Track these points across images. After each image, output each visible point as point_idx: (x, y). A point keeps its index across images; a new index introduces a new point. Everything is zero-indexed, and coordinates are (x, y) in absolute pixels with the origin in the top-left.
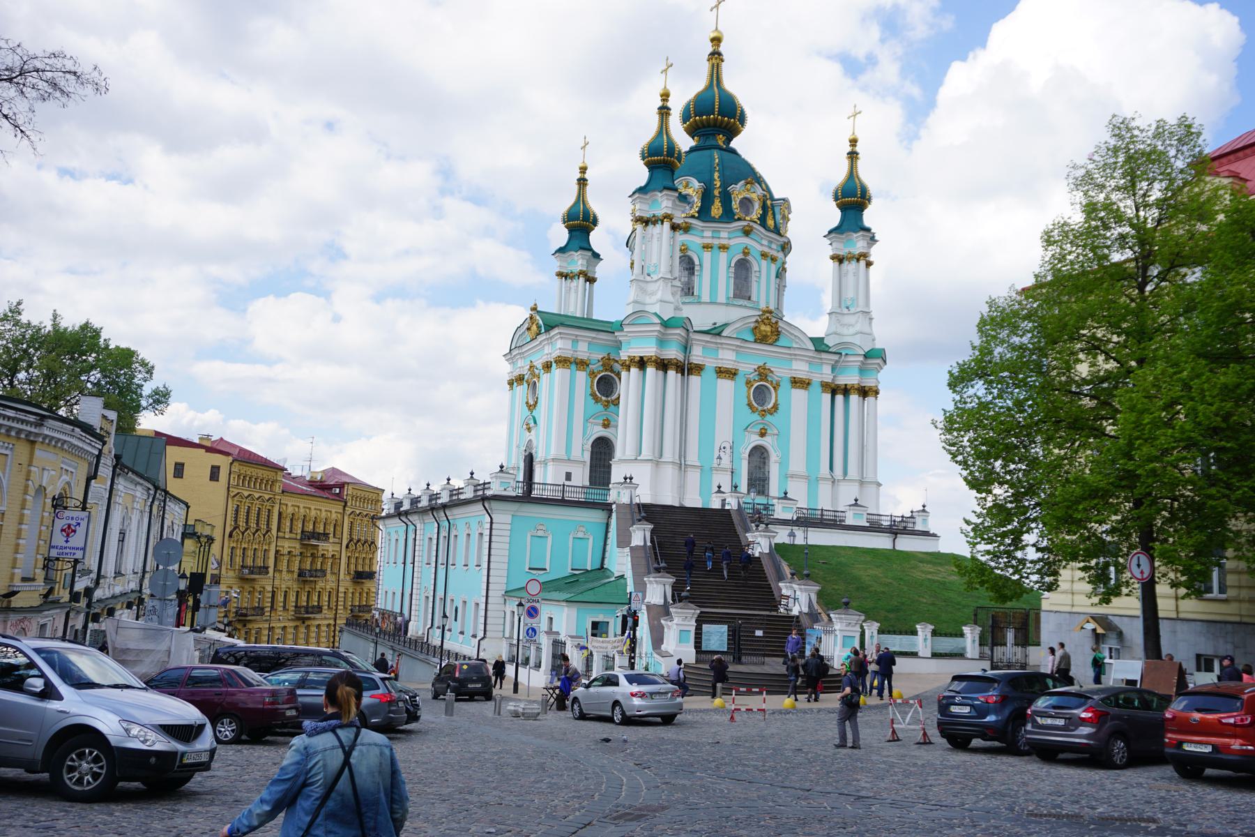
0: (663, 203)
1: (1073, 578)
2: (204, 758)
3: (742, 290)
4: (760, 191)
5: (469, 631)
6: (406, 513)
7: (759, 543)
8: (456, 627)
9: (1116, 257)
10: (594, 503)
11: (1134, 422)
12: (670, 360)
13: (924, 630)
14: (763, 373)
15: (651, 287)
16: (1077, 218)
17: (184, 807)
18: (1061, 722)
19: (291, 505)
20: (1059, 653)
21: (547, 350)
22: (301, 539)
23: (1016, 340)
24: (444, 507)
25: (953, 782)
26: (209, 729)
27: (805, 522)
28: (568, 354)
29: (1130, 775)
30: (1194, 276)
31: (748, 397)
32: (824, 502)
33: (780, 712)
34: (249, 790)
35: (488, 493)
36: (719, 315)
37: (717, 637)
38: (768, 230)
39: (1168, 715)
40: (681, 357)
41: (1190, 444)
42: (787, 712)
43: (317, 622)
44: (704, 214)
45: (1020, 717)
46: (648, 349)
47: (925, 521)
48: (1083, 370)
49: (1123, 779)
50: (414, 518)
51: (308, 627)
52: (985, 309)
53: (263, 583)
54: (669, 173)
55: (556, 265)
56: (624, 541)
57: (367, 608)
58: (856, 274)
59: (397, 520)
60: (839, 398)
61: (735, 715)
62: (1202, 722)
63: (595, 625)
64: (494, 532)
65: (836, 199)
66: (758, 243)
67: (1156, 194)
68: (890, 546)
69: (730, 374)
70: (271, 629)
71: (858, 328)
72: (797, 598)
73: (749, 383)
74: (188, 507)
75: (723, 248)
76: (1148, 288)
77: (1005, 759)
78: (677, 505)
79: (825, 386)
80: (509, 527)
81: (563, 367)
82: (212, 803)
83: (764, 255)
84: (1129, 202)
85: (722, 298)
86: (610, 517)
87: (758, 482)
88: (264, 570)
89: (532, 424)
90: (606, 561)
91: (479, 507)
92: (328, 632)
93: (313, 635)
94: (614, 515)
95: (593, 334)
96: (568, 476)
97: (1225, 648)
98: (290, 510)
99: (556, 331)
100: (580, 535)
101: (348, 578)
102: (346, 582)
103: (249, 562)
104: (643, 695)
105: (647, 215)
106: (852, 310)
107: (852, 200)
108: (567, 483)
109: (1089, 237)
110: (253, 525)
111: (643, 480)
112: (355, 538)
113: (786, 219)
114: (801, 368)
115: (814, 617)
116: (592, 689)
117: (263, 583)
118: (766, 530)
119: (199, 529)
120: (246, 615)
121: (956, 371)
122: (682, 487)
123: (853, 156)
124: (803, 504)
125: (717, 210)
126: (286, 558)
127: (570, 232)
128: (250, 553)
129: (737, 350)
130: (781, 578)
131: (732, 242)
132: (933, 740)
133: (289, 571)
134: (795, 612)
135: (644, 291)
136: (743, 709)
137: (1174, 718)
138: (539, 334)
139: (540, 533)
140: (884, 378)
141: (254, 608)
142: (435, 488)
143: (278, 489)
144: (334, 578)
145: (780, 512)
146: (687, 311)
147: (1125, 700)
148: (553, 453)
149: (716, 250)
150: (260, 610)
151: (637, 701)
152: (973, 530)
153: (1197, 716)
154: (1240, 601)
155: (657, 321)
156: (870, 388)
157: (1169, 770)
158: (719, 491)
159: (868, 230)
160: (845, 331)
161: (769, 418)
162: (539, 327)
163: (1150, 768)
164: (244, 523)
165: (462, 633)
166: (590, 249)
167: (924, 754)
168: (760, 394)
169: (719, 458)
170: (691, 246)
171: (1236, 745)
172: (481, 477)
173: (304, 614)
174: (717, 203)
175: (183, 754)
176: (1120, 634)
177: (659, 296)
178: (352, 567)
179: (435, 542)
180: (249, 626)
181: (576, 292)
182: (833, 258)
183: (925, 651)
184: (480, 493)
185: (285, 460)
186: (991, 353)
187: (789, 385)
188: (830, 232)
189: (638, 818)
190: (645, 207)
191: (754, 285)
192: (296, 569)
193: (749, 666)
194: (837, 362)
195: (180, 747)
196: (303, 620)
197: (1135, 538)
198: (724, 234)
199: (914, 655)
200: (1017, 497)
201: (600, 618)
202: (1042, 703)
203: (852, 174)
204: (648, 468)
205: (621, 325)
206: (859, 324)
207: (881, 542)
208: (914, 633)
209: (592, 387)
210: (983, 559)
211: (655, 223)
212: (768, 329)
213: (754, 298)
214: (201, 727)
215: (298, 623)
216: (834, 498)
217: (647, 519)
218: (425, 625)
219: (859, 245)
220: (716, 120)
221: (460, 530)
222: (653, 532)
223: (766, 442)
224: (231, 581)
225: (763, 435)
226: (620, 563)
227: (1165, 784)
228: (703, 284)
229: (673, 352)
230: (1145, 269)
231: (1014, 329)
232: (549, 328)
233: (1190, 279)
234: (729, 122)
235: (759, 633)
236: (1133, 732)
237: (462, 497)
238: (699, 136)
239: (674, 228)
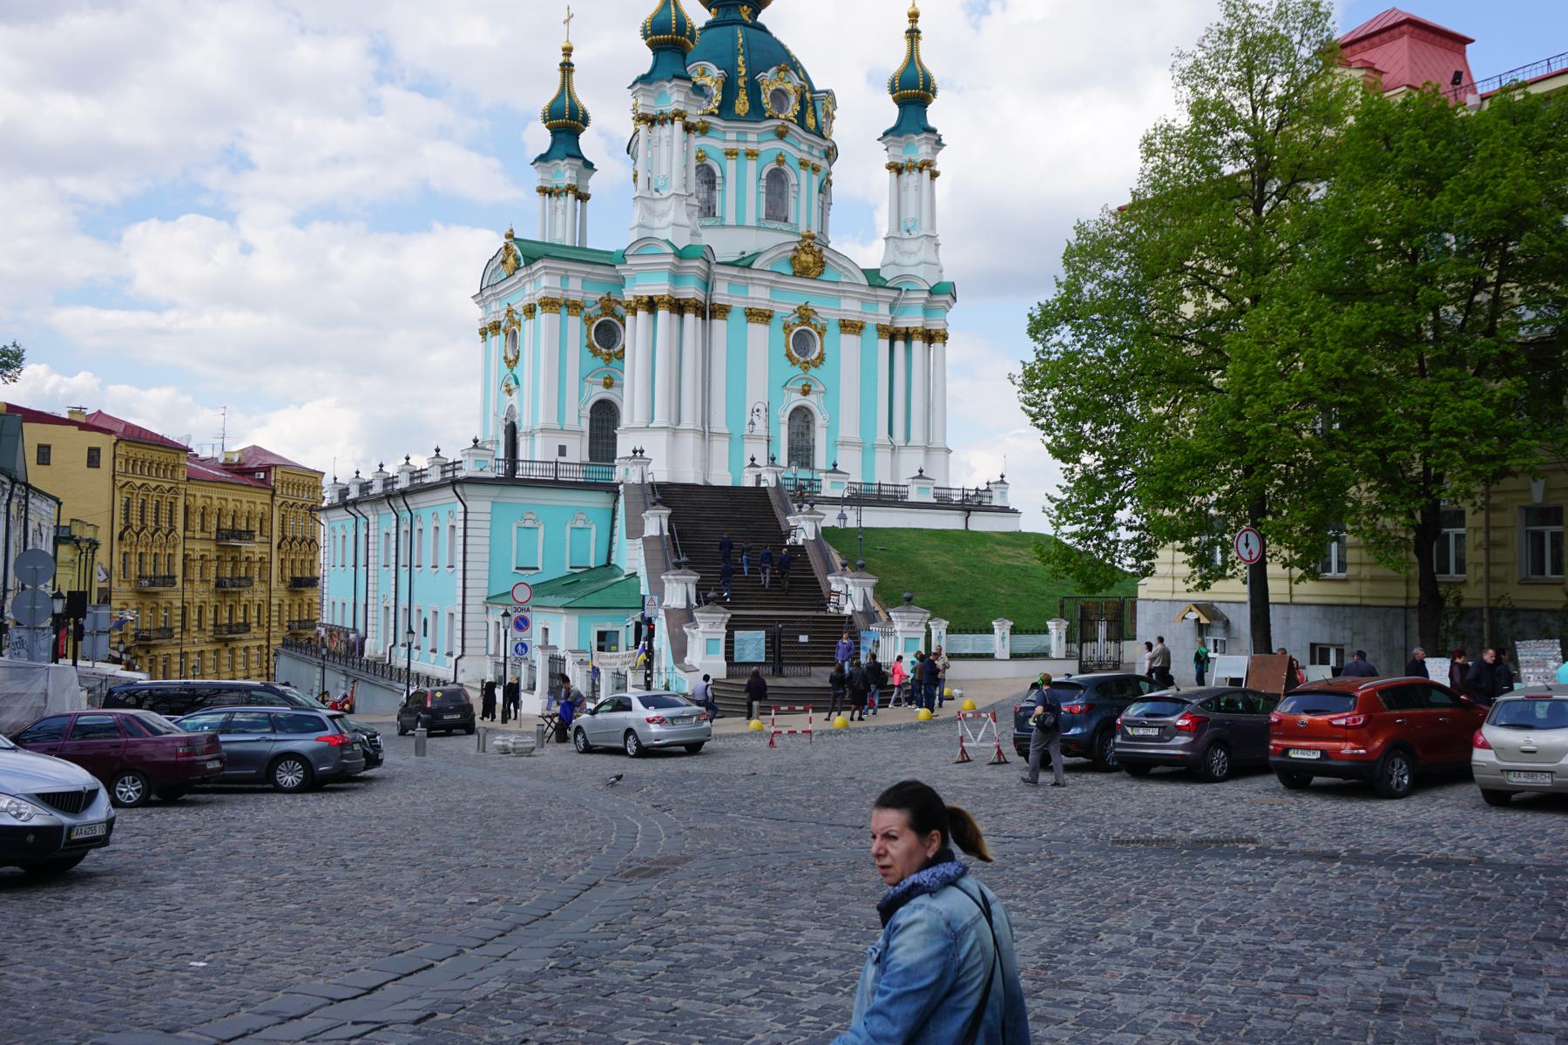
0: (673, 97)
1: (1172, 561)
2: (100, 831)
3: (776, 209)
4: (796, 81)
5: (443, 648)
6: (355, 503)
7: (803, 528)
8: (427, 643)
9: (1228, 169)
10: (595, 484)
11: (1244, 374)
12: (687, 301)
13: (1001, 628)
14: (805, 315)
15: (661, 207)
16: (1184, 121)
17: (77, 894)
18: (1154, 732)
19: (200, 495)
20: (1157, 648)
21: (529, 289)
22: (217, 539)
23: (1109, 274)
24: (404, 493)
25: (1030, 808)
26: (103, 796)
27: (860, 499)
28: (557, 294)
29: (1231, 789)
30: (1318, 192)
31: (787, 346)
32: (882, 475)
33: (830, 733)
34: (162, 866)
35: (460, 474)
36: (749, 242)
37: (752, 645)
38: (808, 131)
39: (1274, 719)
40: (701, 296)
41: (1308, 399)
42: (838, 732)
43: (244, 644)
44: (726, 110)
45: (1108, 728)
46: (659, 286)
47: (1003, 494)
48: (1188, 310)
49: (1222, 793)
50: (365, 509)
51: (232, 651)
52: (1072, 237)
53: (170, 596)
54: (679, 56)
55: (536, 177)
56: (635, 531)
57: (311, 624)
58: (918, 188)
59: (343, 512)
60: (900, 345)
61: (776, 739)
62: (1311, 725)
63: (602, 636)
64: (469, 524)
65: (893, 91)
66: (795, 149)
67: (1276, 91)
68: (962, 527)
70: (183, 655)
71: (921, 256)
72: (850, 593)
74: (60, 504)
75: (751, 154)
76: (1265, 208)
77: (1090, 777)
78: (701, 483)
79: (882, 330)
80: (488, 517)
81: (550, 311)
82: (114, 886)
83: (803, 164)
84: (1245, 101)
85: (751, 220)
86: (616, 500)
87: (801, 452)
88: (169, 580)
89: (513, 385)
90: (614, 556)
91: (449, 492)
92: (260, 656)
93: (241, 660)
94: (622, 498)
95: (588, 268)
96: (562, 451)
97: (1341, 635)
98: (200, 502)
99: (539, 264)
100: (580, 524)
101: (282, 586)
102: (280, 592)
103: (149, 571)
104: (661, 721)
105: (651, 112)
106: (914, 234)
107: (913, 93)
108: (561, 459)
109: (1196, 144)
110: (150, 523)
111: (657, 452)
112: (289, 535)
113: (830, 117)
114: (851, 309)
115: (870, 616)
116: (599, 716)
117: (170, 596)
118: (811, 511)
119: (77, 531)
120: (149, 639)
121: (1037, 314)
122: (706, 461)
123: (913, 35)
124: (856, 477)
125: (742, 105)
126: (198, 564)
127: (554, 134)
128: (149, 559)
129: (772, 286)
130: (830, 570)
131: (763, 147)
132: (1009, 758)
133: (203, 581)
134: (848, 611)
135: (651, 212)
136: (785, 731)
137: (1280, 721)
138: (518, 268)
139: (529, 524)
140: (954, 320)
141: (159, 630)
142: (391, 470)
143: (181, 475)
144: (263, 587)
145: (829, 489)
146: (708, 238)
147: (1227, 702)
148: (541, 421)
149: (742, 157)
150: (167, 632)
151: (654, 729)
152: (1057, 508)
153: (1305, 718)
154: (1361, 580)
155: (669, 250)
156: (937, 332)
157: (1273, 781)
158: (752, 465)
159: (933, 131)
160: (906, 260)
161: (813, 371)
162: (517, 259)
163: (1252, 779)
164: (141, 520)
165: (434, 651)
166: (581, 157)
167: (999, 775)
168: (802, 342)
169: (752, 423)
171: (1347, 749)
172: (450, 455)
173: (226, 635)
174: (743, 96)
175: (71, 828)
176: (1227, 623)
177: (671, 218)
178: (288, 572)
179: (393, 538)
180: (155, 652)
181: (564, 213)
182: (889, 167)
183: (1002, 651)
184: (450, 475)
185: (189, 438)
186: (1079, 290)
187: (837, 330)
188: (885, 134)
189: (655, 873)
190: (650, 102)
191: (792, 203)
192: (212, 576)
193: (793, 679)
194: (896, 299)
195: (66, 820)
196: (226, 642)
197: (1244, 512)
198: (752, 137)
199: (990, 657)
200: (1110, 467)
201: (608, 627)
202: (1133, 711)
203: (913, 58)
204: (663, 437)
205: (623, 257)
206: (921, 251)
207: (951, 521)
208: (990, 631)
209: (588, 336)
210: (1069, 542)
211: (662, 122)
212: (810, 258)
213: (792, 219)
214: (92, 795)
215: (219, 646)
216: (894, 469)
217: (664, 503)
218: (386, 642)
219: (921, 151)
221: (426, 522)
222: (670, 518)
223: (811, 401)
224: (125, 597)
225: (805, 392)
226: (631, 557)
227: (1268, 797)
228: (726, 200)
229: (690, 291)
230: (1262, 184)
231: (1107, 261)
232: (530, 260)
233: (1313, 197)
235: (803, 638)
236: (1235, 739)
237: (426, 481)
238: (717, 7)
239: (688, 128)
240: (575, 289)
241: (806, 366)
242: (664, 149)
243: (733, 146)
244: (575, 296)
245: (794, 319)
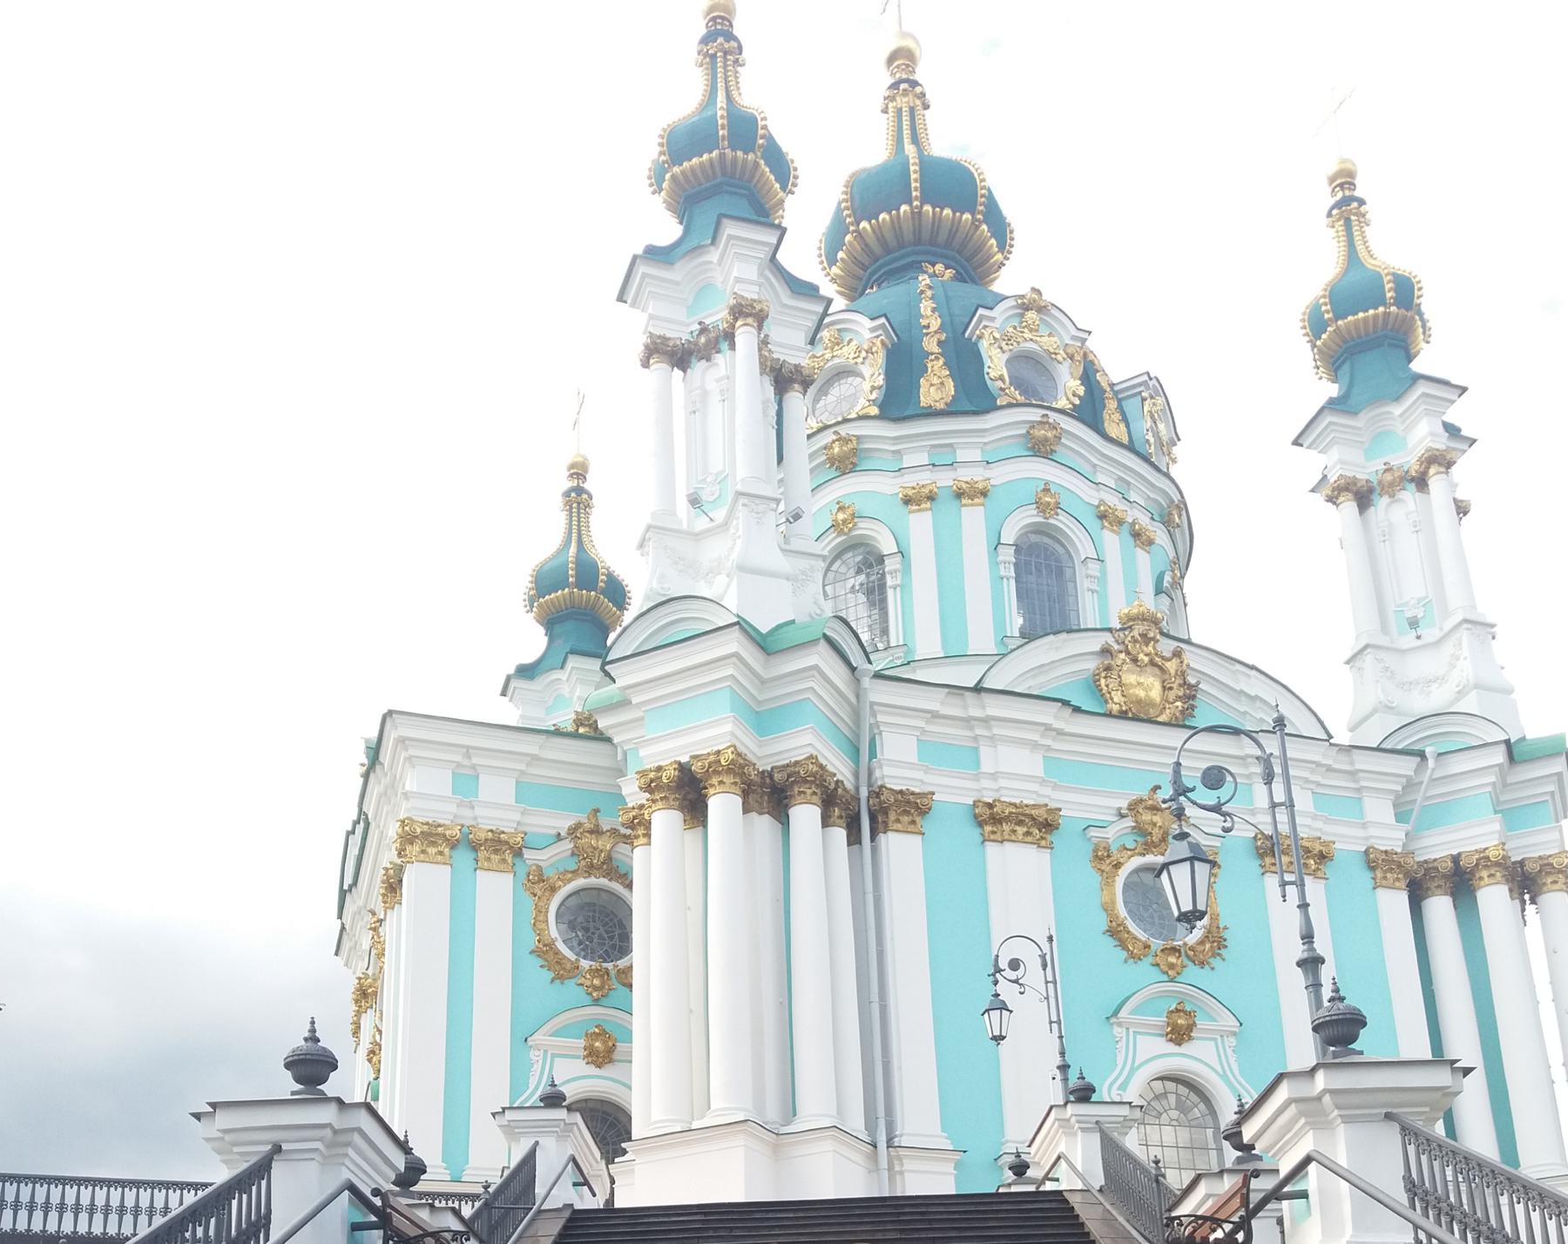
12: (791, 770)
28: (445, 812)
31: (1108, 908)
40: (840, 768)
46: (707, 732)
66: (1085, 477)
69: (1039, 825)
73: (1103, 858)
106: (1430, 634)
131: (1000, 475)
149: (946, 505)
170: (860, 506)
194: (1410, 785)
220: (917, 215)
229: (802, 743)
234: (956, 225)
241: (1173, 960)
242: (716, 410)
243: (924, 478)
245: (1117, 833)
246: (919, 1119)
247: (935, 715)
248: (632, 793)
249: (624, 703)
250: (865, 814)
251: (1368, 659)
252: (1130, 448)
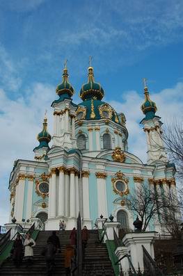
14: (119, 176)
15: (61, 139)
40: (77, 168)
44: (88, 117)
60: (158, 186)
65: (143, 108)
73: (113, 180)
85: (99, 149)
114: (137, 173)
125: (93, 116)
135: (58, 141)
149: (94, 130)
161: (125, 196)
191: (112, 144)
203: (147, 100)
209: (36, 188)
212: (119, 156)
239: (72, 117)
240: (31, 171)
244: (31, 174)
246: (86, 216)
247: (90, 161)
248: (49, 170)
249: (49, 159)
250: (80, 174)
251: (149, 153)
252: (119, 124)
